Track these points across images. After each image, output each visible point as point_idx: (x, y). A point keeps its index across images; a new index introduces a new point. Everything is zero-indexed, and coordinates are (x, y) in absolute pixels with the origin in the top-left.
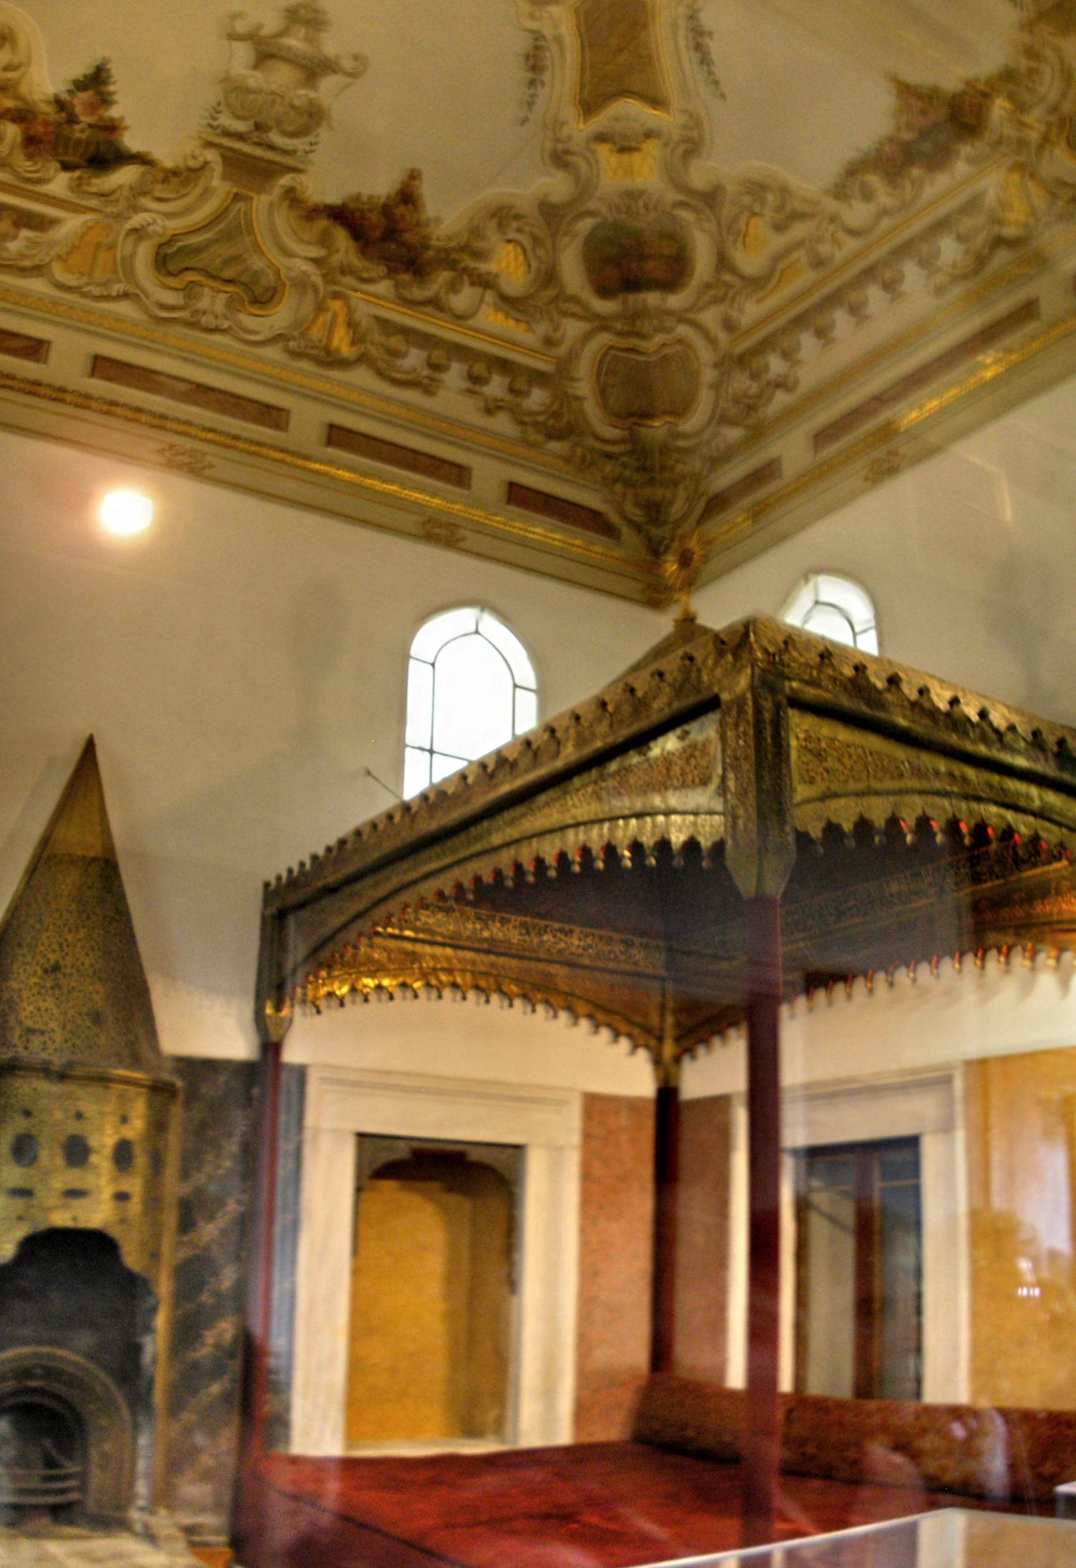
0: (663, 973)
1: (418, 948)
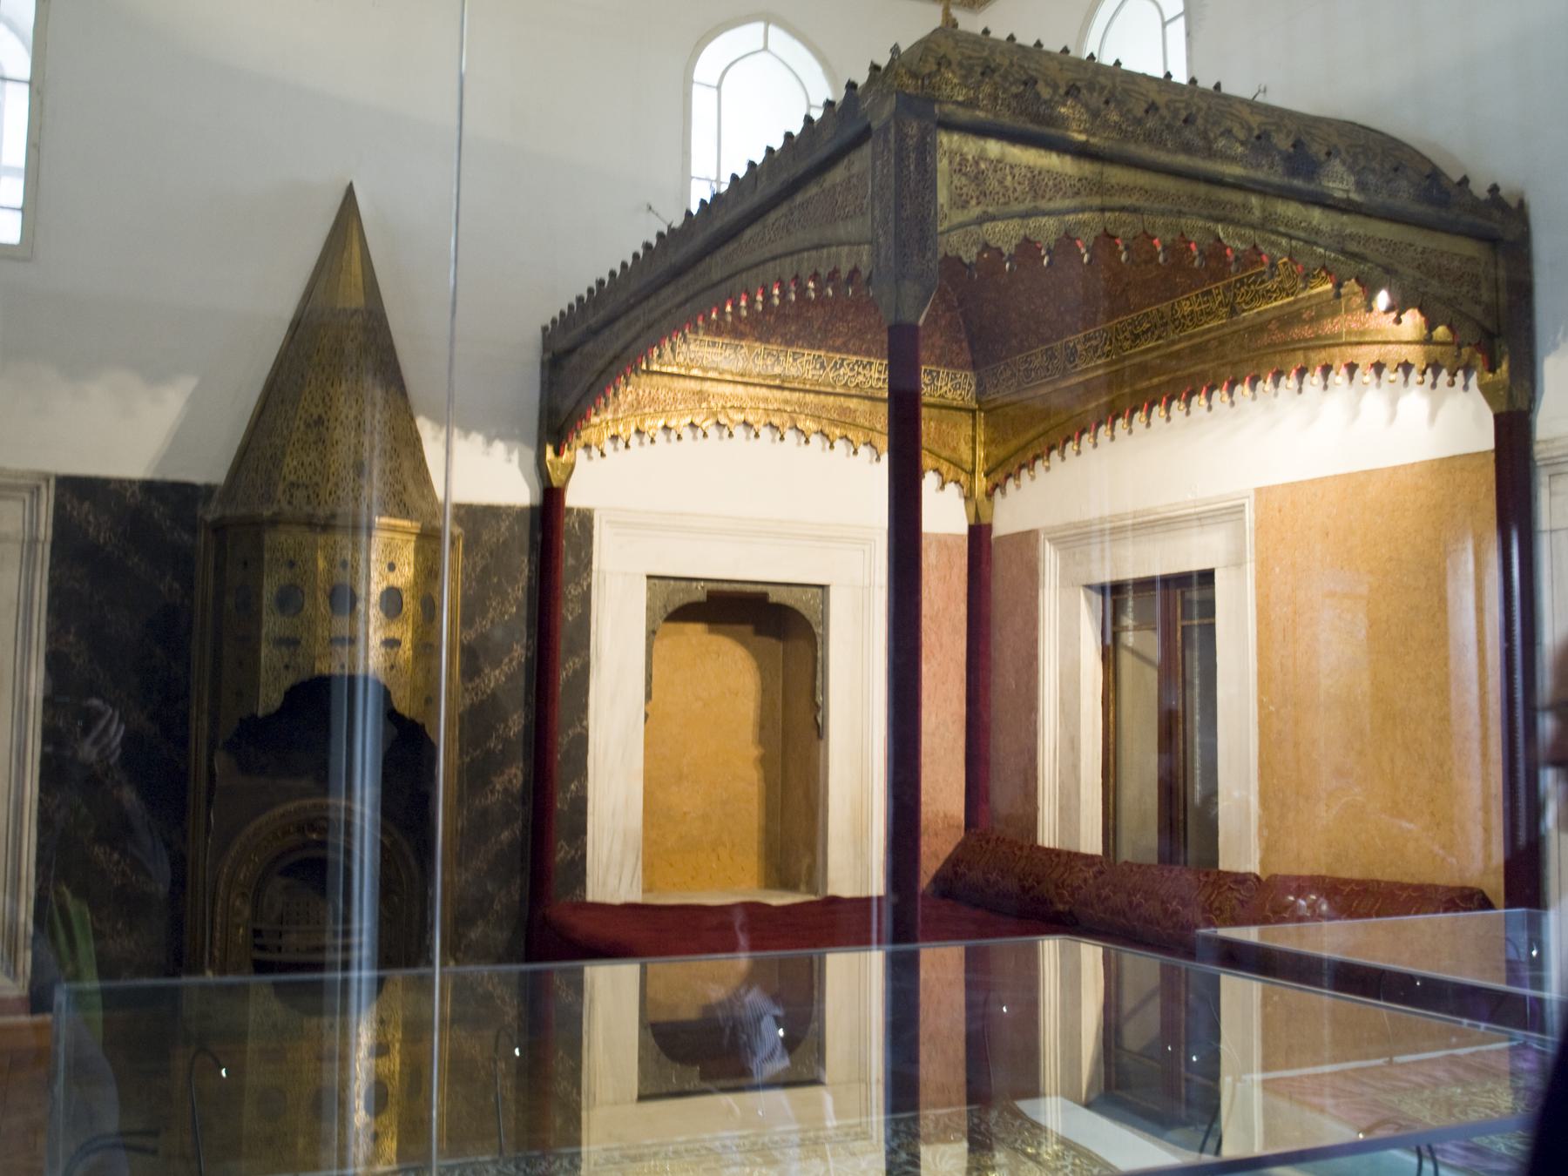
0: (974, 405)
1: (707, 386)
